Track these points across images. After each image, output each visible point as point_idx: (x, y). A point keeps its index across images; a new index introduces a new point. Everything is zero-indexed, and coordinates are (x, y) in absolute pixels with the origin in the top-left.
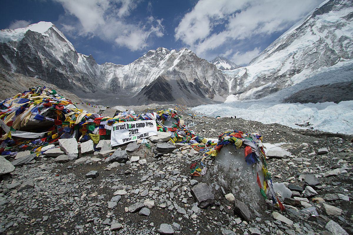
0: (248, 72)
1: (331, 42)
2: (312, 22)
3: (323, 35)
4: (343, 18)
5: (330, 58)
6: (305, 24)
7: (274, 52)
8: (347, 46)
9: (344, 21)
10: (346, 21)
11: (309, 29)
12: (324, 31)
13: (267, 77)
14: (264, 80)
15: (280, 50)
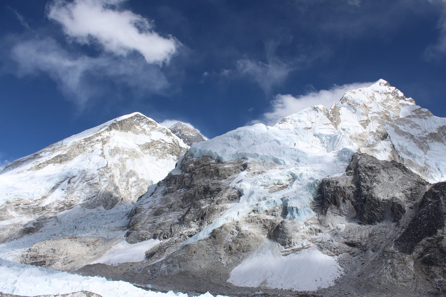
1: (119, 173)
2: (105, 137)
3: (112, 161)
8: (133, 185)
9: (138, 150)
11: (99, 146)
12: (115, 155)
14: (16, 208)
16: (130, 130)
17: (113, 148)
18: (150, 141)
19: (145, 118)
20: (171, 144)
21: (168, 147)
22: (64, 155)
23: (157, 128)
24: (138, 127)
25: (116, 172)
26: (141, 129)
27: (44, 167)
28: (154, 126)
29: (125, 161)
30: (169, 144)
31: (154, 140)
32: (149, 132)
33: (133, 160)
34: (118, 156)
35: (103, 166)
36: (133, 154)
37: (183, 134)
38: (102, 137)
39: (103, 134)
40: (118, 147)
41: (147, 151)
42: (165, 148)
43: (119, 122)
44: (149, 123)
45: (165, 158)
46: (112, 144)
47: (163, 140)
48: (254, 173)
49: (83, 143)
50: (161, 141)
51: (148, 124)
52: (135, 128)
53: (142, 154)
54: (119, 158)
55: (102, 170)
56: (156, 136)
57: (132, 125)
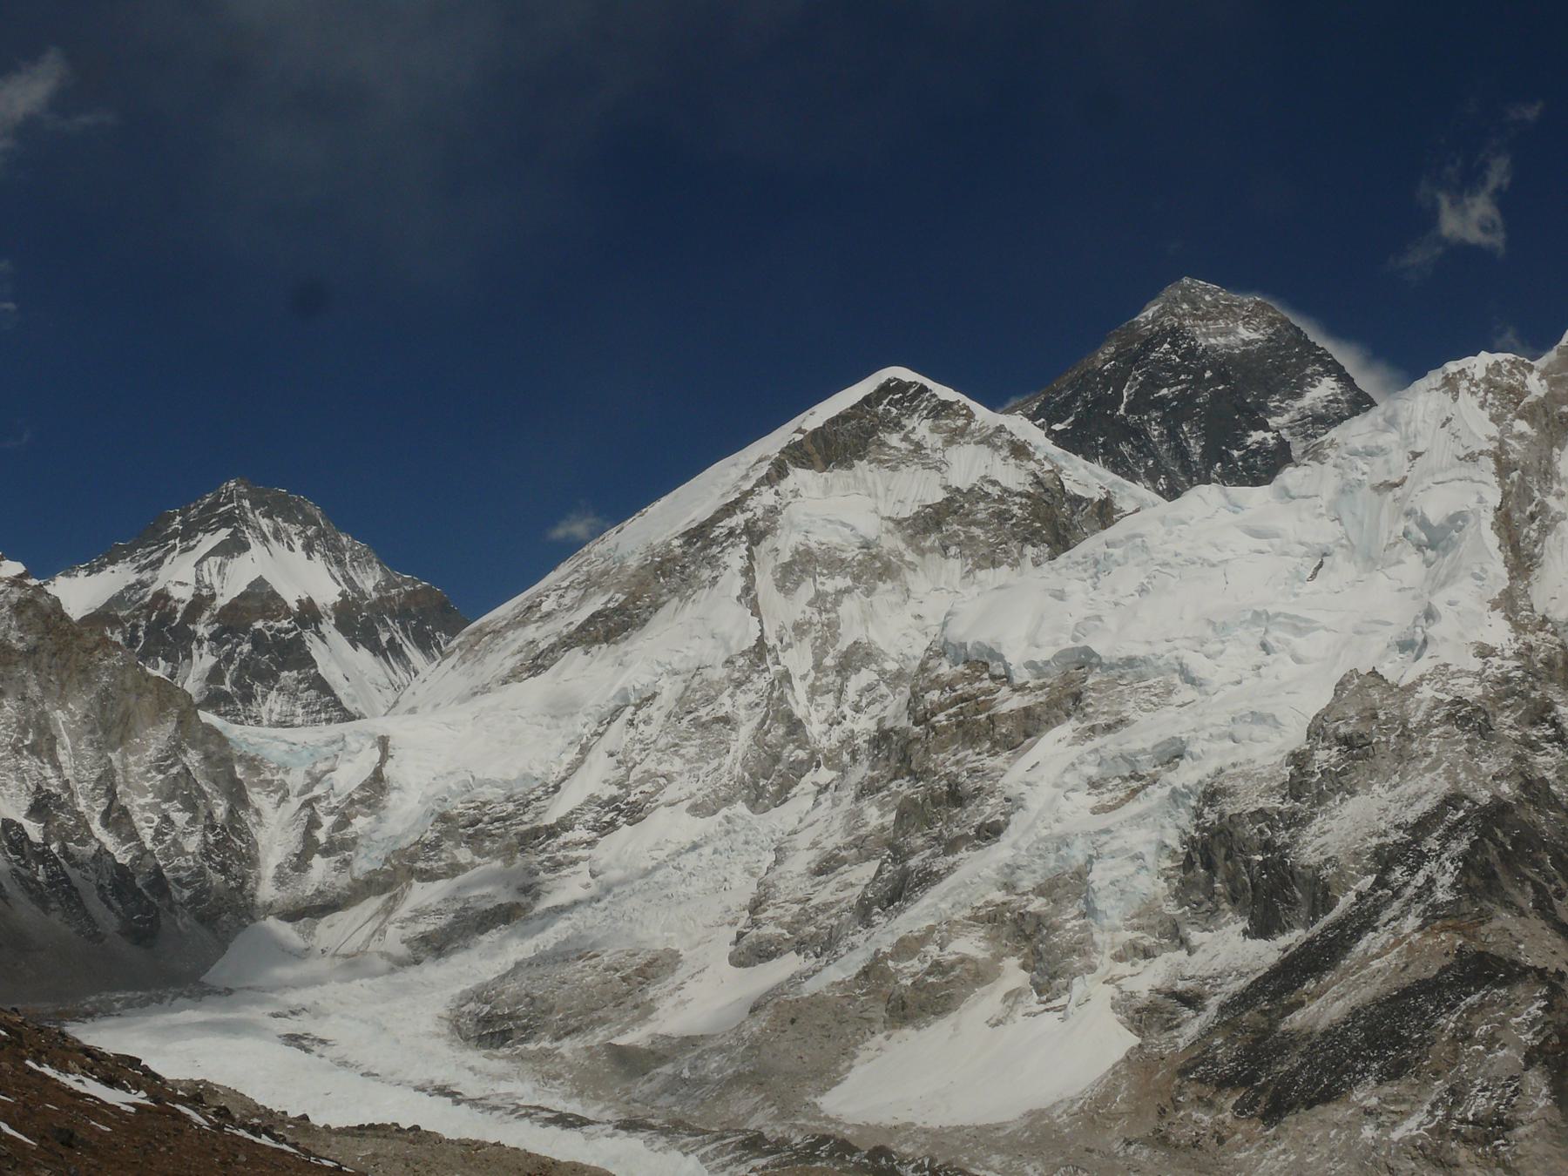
0: (387, 771)
2: (760, 512)
4: (898, 523)
5: (777, 759)
6: (728, 510)
7: (567, 643)
8: (864, 703)
9: (893, 543)
10: (902, 546)
12: (797, 584)
13: (486, 819)
15: (596, 640)
16: (861, 458)
17: (787, 559)
18: (940, 496)
19: (923, 389)
21: (1016, 510)
22: (615, 610)
24: (894, 439)
25: (798, 660)
26: (903, 445)
27: (555, 660)
28: (961, 422)
29: (837, 603)
30: (1020, 494)
31: (958, 489)
32: (939, 455)
33: (869, 592)
34: (806, 591)
35: (745, 648)
36: (874, 569)
37: (1191, 353)
38: (749, 515)
39: (751, 503)
40: (808, 551)
41: (932, 540)
42: (1002, 516)
43: (815, 432)
45: (1001, 564)
46: (785, 542)
47: (994, 483)
48: (1093, 729)
49: (678, 551)
50: (989, 489)
51: (936, 417)
52: (882, 444)
53: (910, 556)
54: (812, 594)
55: (740, 662)
56: (969, 465)
57: (873, 431)
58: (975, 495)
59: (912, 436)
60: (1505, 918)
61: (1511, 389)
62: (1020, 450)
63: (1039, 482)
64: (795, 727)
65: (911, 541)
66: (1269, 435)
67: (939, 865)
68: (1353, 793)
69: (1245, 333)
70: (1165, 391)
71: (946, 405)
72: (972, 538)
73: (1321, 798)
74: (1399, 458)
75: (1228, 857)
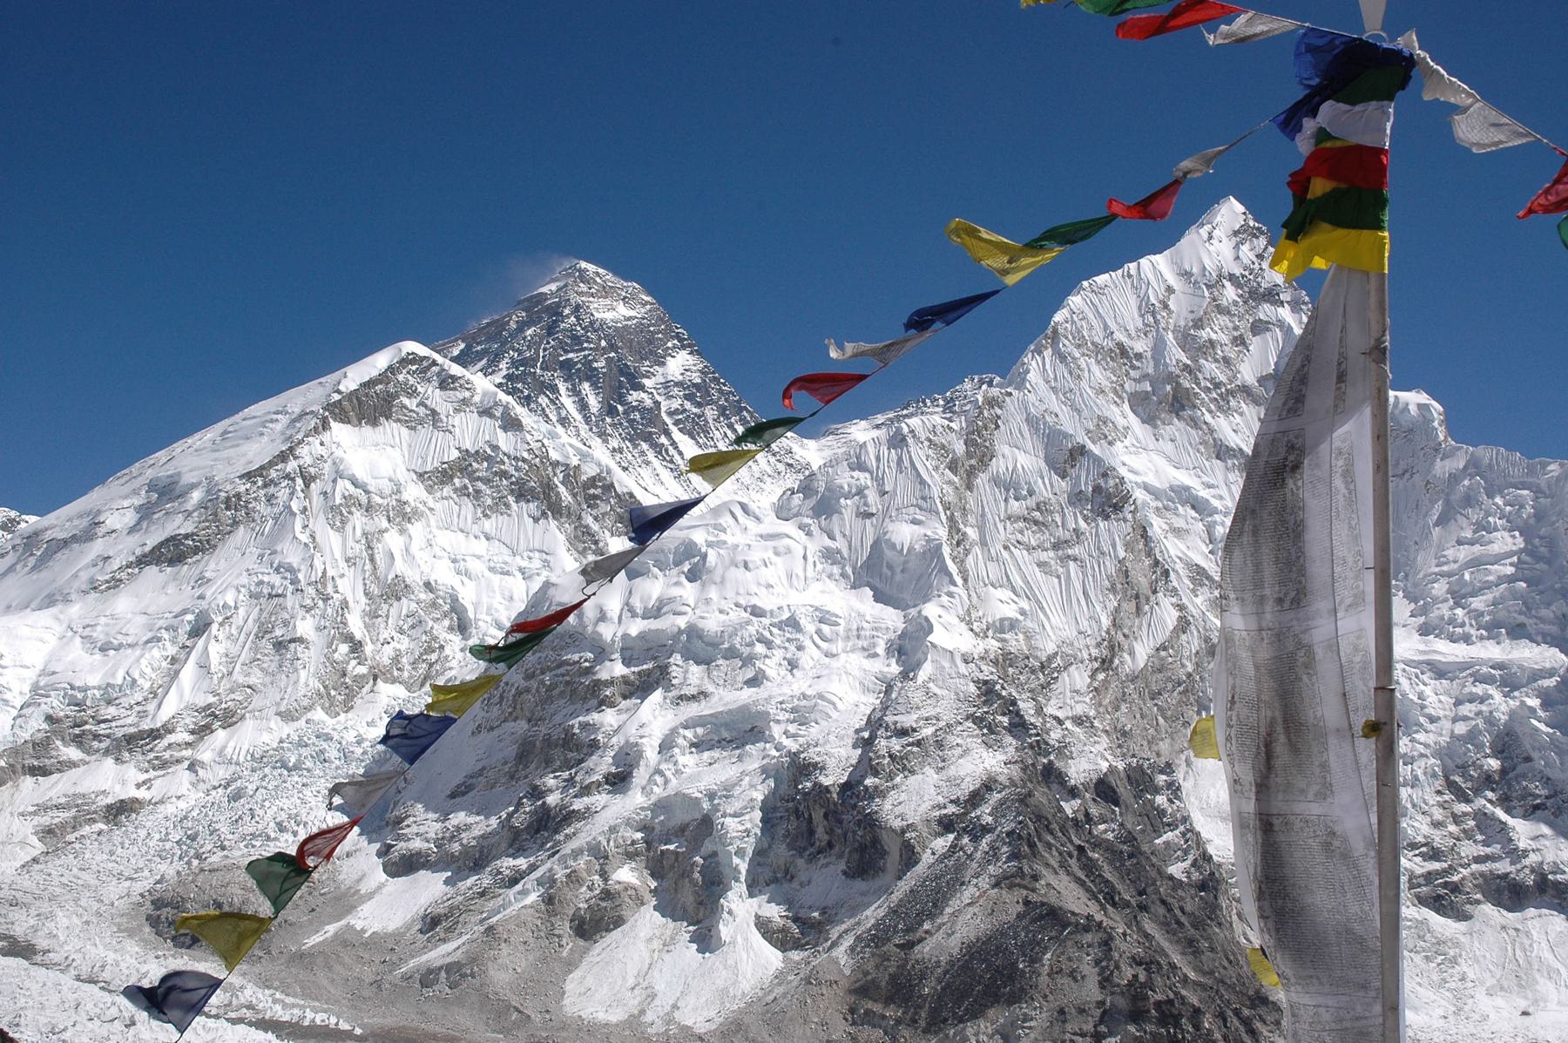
19: (434, 363)
20: (524, 460)
23: (477, 399)
26: (422, 411)
28: (467, 394)
30: (516, 458)
41: (447, 491)
42: (504, 474)
44: (446, 382)
47: (495, 448)
58: (478, 455)
59: (428, 403)
60: (1048, 877)
61: (943, 447)
62: (511, 424)
63: (530, 451)
64: (356, 647)
65: (430, 490)
66: (644, 395)
67: (578, 805)
68: (912, 772)
69: (623, 311)
70: (571, 355)
71: (454, 378)
72: (478, 492)
73: (891, 777)
74: (872, 496)
75: (826, 816)
